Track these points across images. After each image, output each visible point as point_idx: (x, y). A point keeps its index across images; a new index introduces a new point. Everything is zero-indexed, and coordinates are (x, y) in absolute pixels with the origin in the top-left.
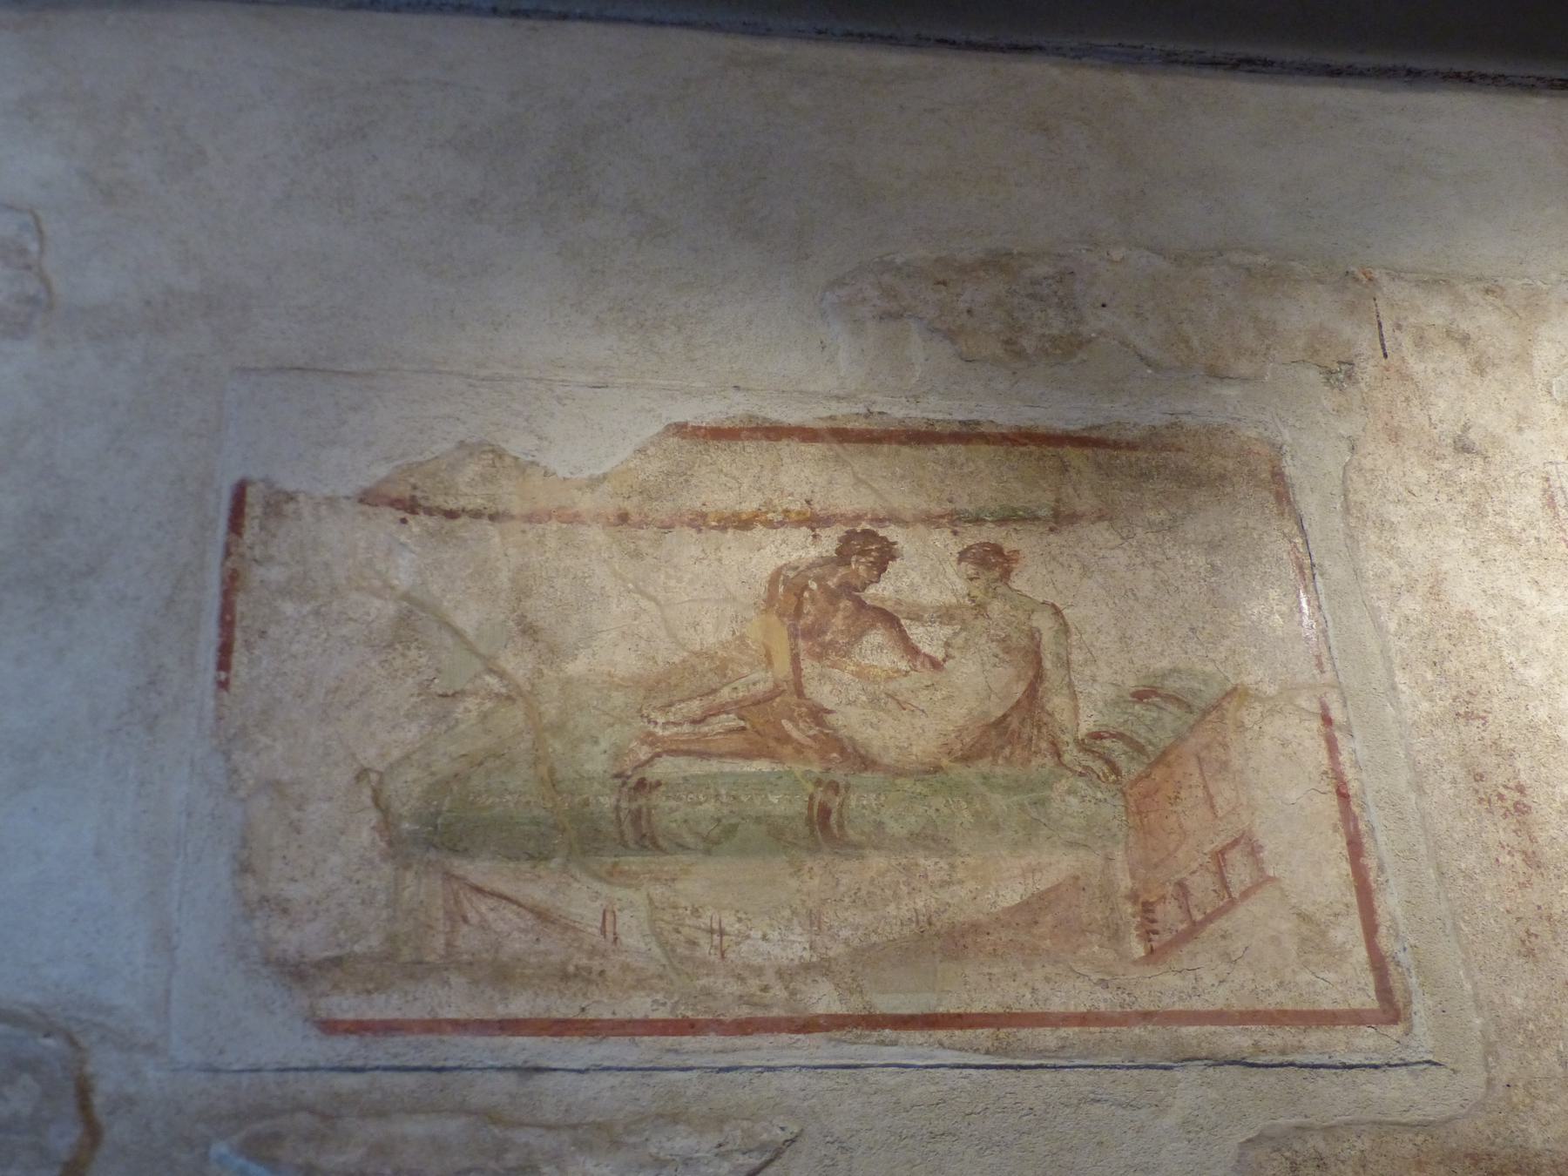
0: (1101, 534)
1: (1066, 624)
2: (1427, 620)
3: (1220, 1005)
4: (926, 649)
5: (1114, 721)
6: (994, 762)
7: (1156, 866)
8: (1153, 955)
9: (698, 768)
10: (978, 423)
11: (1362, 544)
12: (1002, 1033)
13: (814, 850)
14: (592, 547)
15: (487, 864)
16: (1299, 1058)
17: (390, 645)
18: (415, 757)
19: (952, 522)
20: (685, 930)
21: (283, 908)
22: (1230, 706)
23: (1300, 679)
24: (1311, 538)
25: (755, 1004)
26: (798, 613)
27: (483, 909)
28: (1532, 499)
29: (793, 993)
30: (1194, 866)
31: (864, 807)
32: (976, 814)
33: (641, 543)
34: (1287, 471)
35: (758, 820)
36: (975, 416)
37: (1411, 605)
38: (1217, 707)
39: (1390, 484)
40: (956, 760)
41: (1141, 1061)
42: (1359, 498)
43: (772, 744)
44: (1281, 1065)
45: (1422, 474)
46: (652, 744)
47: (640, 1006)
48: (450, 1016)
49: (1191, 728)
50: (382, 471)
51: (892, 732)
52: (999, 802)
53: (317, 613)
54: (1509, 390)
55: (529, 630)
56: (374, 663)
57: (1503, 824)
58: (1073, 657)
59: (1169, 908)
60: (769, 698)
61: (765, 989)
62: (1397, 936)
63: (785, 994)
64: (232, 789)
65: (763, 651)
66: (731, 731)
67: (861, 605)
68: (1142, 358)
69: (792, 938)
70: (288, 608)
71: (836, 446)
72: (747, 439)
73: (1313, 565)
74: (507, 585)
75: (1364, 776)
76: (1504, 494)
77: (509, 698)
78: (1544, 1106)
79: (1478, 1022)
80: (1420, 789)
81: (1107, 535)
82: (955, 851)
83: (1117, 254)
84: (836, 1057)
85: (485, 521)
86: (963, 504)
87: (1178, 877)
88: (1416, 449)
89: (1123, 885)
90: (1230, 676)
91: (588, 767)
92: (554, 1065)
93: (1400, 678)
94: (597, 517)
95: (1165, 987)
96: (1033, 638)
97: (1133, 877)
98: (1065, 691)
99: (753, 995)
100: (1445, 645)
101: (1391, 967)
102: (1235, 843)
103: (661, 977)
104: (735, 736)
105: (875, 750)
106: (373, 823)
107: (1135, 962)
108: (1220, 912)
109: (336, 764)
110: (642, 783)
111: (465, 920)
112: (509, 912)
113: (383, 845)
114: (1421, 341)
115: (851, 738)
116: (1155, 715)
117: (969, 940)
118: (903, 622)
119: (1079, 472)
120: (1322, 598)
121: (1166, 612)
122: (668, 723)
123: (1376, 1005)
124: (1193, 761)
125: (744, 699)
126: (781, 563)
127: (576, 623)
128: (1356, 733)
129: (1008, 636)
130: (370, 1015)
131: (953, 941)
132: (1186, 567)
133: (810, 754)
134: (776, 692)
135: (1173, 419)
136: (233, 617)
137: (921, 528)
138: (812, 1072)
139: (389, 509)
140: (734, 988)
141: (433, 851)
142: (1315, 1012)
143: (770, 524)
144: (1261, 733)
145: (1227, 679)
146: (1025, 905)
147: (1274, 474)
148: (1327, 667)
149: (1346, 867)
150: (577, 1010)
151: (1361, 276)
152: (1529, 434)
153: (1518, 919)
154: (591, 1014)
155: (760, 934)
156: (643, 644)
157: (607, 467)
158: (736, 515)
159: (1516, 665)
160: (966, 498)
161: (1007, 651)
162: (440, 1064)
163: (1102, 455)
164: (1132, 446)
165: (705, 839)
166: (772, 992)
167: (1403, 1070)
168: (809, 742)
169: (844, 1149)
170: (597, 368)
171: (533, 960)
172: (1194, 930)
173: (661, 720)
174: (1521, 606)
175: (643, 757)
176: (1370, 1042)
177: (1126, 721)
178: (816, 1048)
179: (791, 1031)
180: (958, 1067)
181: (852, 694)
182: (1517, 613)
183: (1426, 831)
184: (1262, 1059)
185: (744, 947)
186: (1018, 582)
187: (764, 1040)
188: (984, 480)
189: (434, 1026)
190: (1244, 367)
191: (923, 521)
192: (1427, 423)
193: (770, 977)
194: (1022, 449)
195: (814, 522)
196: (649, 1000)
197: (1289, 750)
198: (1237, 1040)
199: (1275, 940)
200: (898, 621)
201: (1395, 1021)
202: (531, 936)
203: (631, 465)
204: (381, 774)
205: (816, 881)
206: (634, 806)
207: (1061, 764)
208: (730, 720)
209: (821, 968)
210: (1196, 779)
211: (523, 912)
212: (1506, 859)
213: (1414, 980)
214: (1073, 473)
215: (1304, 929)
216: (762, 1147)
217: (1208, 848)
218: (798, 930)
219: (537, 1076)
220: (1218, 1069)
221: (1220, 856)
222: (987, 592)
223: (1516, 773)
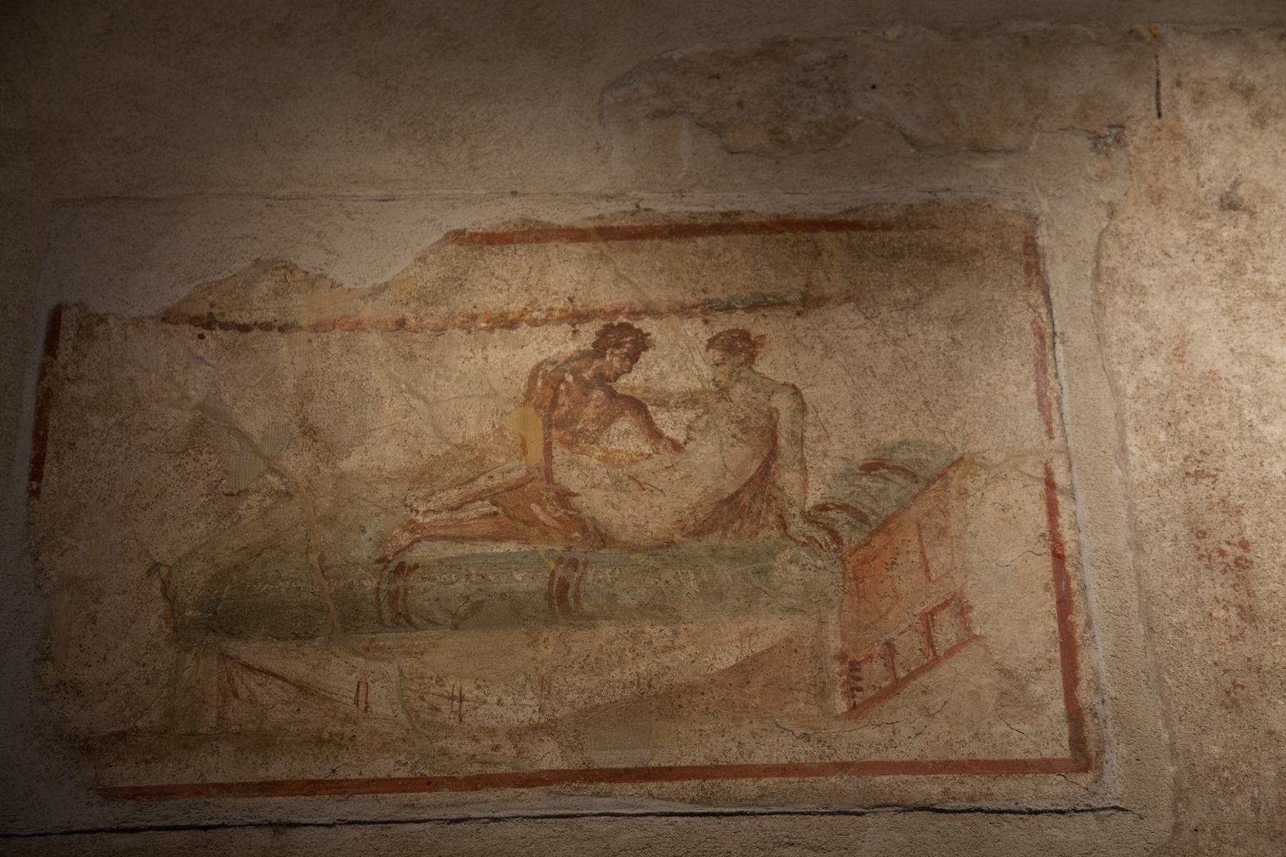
0: (847, 316)
1: (803, 403)
2: (1167, 382)
3: (914, 755)
4: (669, 433)
5: (841, 493)
6: (724, 535)
7: (867, 627)
9: (452, 551)
10: (738, 213)
11: (1109, 310)
12: (707, 784)
14: (371, 352)
15: (258, 644)
16: (985, 804)
17: (185, 451)
18: (201, 551)
19: (704, 312)
20: (429, 698)
22: (955, 475)
23: (1028, 445)
24: (1055, 307)
25: (484, 763)
26: (554, 404)
30: (903, 626)
31: (599, 581)
32: (702, 585)
33: (416, 346)
34: (1040, 242)
35: (503, 596)
36: (736, 207)
37: (1152, 368)
39: (1147, 248)
40: (689, 535)
42: (1111, 264)
43: (521, 527)
44: (969, 811)
45: (1181, 235)
46: (412, 531)
47: (384, 767)
48: (216, 781)
49: (915, 497)
50: (184, 291)
51: (631, 511)
52: (725, 573)
53: (120, 424)
55: (310, 432)
56: (169, 468)
57: (1221, 579)
58: (807, 434)
59: (875, 667)
61: (496, 748)
62: (1097, 689)
63: (514, 752)
64: (39, 587)
65: (519, 441)
66: (484, 516)
67: (612, 394)
68: (906, 137)
69: (524, 702)
70: (96, 421)
71: (602, 245)
72: (520, 241)
73: (1054, 334)
75: (1082, 537)
76: (1267, 250)
77: (287, 494)
78: (1232, 850)
79: (1172, 769)
80: (1137, 547)
81: (852, 316)
82: (679, 619)
83: (891, 34)
84: (555, 808)
85: (275, 333)
86: (717, 293)
87: (887, 637)
88: (1179, 210)
89: (833, 646)
90: (957, 445)
91: (353, 554)
92: (304, 821)
93: (1132, 440)
94: (377, 324)
95: (864, 740)
96: (771, 418)
97: (844, 638)
98: (797, 467)
99: (485, 754)
100: (1183, 405)
101: (1088, 719)
102: (946, 603)
103: (404, 740)
104: (487, 521)
105: (615, 530)
106: (160, 612)
107: (837, 718)
108: (924, 669)
109: (131, 561)
110: (402, 566)
111: (236, 695)
112: (275, 686)
113: (168, 630)
114: (1200, 99)
115: (593, 519)
116: (880, 486)
117: (684, 701)
118: (649, 408)
119: (831, 255)
120: (1060, 365)
121: (902, 387)
122: (429, 511)
123: (1068, 755)
124: (914, 526)
125: (500, 486)
126: (541, 358)
129: (748, 417)
131: (665, 702)
132: (926, 343)
133: (555, 535)
134: (528, 478)
135: (931, 197)
136: (46, 431)
137: (675, 319)
138: (532, 823)
139: (187, 326)
141: (212, 635)
142: (1006, 762)
143: (534, 323)
145: (955, 449)
146: (740, 667)
147: (1026, 245)
148: (1057, 433)
149: (1053, 625)
150: (329, 771)
151: (1145, 33)
153: (1226, 671)
154: (340, 775)
155: (496, 699)
156: (411, 439)
158: (504, 315)
159: (1255, 422)
160: (719, 287)
162: (205, 823)
163: (856, 237)
164: (887, 227)
165: (453, 615)
166: (502, 750)
167: (1090, 816)
168: (556, 524)
170: (386, 182)
171: (293, 728)
172: (897, 686)
173: (422, 509)
174: (1269, 362)
176: (1059, 789)
177: (852, 493)
178: (536, 800)
179: (516, 786)
180: (665, 815)
181: (598, 477)
182: (1265, 370)
183: (1140, 588)
184: (951, 805)
185: (480, 711)
186: (762, 366)
187: (492, 795)
188: (737, 267)
189: (202, 790)
191: (676, 312)
192: (1194, 181)
194: (778, 236)
195: (576, 318)
196: (392, 761)
197: (1009, 514)
198: (929, 788)
199: (975, 694)
200: (645, 407)
201: (1085, 770)
202: (293, 707)
203: (412, 273)
205: (551, 649)
206: (393, 587)
207: (786, 534)
208: (486, 507)
209: (548, 728)
210: (914, 544)
211: (287, 686)
213: (1109, 730)
214: (825, 257)
215: (1005, 685)
217: (918, 610)
219: (289, 831)
220: (908, 815)
221: (929, 618)
222: (731, 375)
223: (1242, 529)
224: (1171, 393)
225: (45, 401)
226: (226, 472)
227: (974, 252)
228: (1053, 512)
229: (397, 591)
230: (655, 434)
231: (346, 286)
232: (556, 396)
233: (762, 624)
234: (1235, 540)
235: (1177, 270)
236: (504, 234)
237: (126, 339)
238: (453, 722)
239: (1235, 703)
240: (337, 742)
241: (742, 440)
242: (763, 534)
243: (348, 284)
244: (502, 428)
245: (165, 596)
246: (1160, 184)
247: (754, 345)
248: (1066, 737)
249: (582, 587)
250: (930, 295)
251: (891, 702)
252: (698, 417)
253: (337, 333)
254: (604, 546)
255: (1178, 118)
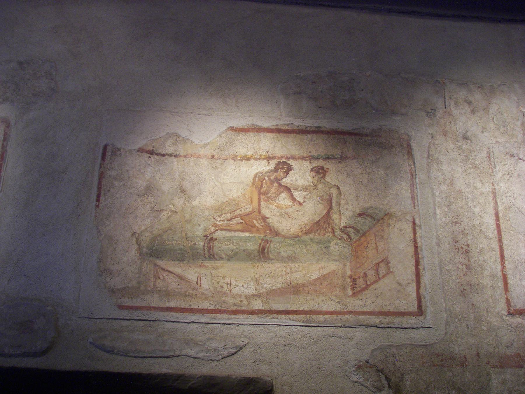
0: (354, 164)
1: (340, 192)
3: (371, 310)
4: (298, 199)
5: (351, 223)
6: (315, 235)
8: (354, 294)
9: (229, 234)
10: (321, 127)
12: (308, 316)
13: (259, 261)
16: (392, 326)
19: (310, 159)
21: (110, 272)
22: (386, 218)
23: (408, 211)
24: (416, 166)
25: (238, 306)
27: (164, 275)
28: (484, 155)
29: (249, 303)
30: (370, 267)
32: (307, 250)
35: (244, 250)
36: (320, 125)
37: (444, 188)
38: (382, 219)
41: (347, 325)
43: (250, 228)
45: (452, 146)
46: (215, 227)
47: (206, 305)
48: (154, 306)
50: (144, 142)
52: (315, 247)
53: (124, 185)
54: (481, 120)
55: (183, 191)
58: (341, 202)
60: (250, 214)
61: (241, 301)
62: (426, 290)
63: (247, 303)
66: (238, 223)
67: (280, 185)
70: (116, 183)
71: (278, 135)
72: (252, 131)
74: (178, 177)
75: (423, 241)
76: (476, 153)
80: (438, 245)
83: (368, 74)
86: (314, 153)
87: (364, 271)
89: (348, 273)
93: (438, 210)
94: (205, 156)
95: (356, 304)
97: (351, 271)
98: (338, 213)
100: (452, 200)
102: (383, 261)
105: (280, 231)
107: (349, 297)
108: (375, 282)
109: (127, 231)
110: (212, 238)
111: (159, 278)
112: (171, 276)
113: (138, 255)
117: (301, 289)
120: (418, 185)
121: (371, 189)
123: (416, 310)
124: (374, 235)
125: (243, 214)
126: (257, 171)
127: (196, 189)
128: (423, 227)
129: (323, 195)
130: (132, 304)
131: (295, 289)
135: (380, 127)
137: (300, 161)
138: (252, 326)
140: (233, 301)
143: (256, 159)
144: (394, 227)
147: (408, 145)
148: (416, 207)
149: (414, 268)
152: (486, 134)
153: (462, 285)
154: (192, 307)
155: (241, 285)
156: (215, 196)
157: (209, 141)
159: (472, 207)
161: (322, 200)
162: (150, 319)
164: (366, 135)
165: (228, 256)
168: (261, 227)
169: (260, 348)
170: (209, 109)
172: (368, 286)
173: (219, 220)
174: (476, 188)
175: (213, 231)
176: (413, 321)
178: (254, 319)
181: (275, 212)
182: (475, 190)
185: (237, 288)
186: (327, 179)
187: (240, 316)
188: (319, 145)
189: (149, 308)
190: (403, 111)
191: (301, 159)
193: (243, 298)
194: (334, 136)
195: (269, 158)
197: (402, 233)
198: (375, 320)
201: (421, 315)
202: (177, 283)
204: (139, 234)
206: (209, 245)
207: (334, 236)
208: (239, 220)
209: (259, 296)
210: (373, 241)
211: (175, 276)
212: (461, 267)
214: (348, 143)
216: (237, 347)
217: (374, 262)
218: (252, 284)
224: (449, 196)
225: (102, 176)
226: (156, 203)
227: (392, 146)
228: (415, 233)
229: (210, 247)
230: (294, 199)
231: (196, 143)
232: (262, 184)
233: (326, 265)
234: (466, 244)
235: (451, 157)
236: (246, 129)
237: (126, 156)
238: (228, 292)
239: (464, 295)
240: (191, 296)
241: (321, 203)
242: (327, 235)
243: (196, 142)
244: (244, 194)
245: (137, 243)
246: (446, 129)
247: (325, 171)
248: (416, 305)
249: (270, 249)
250: (379, 159)
251: (365, 292)
252: (307, 194)
253: (192, 159)
254: (277, 236)
255: (451, 109)
